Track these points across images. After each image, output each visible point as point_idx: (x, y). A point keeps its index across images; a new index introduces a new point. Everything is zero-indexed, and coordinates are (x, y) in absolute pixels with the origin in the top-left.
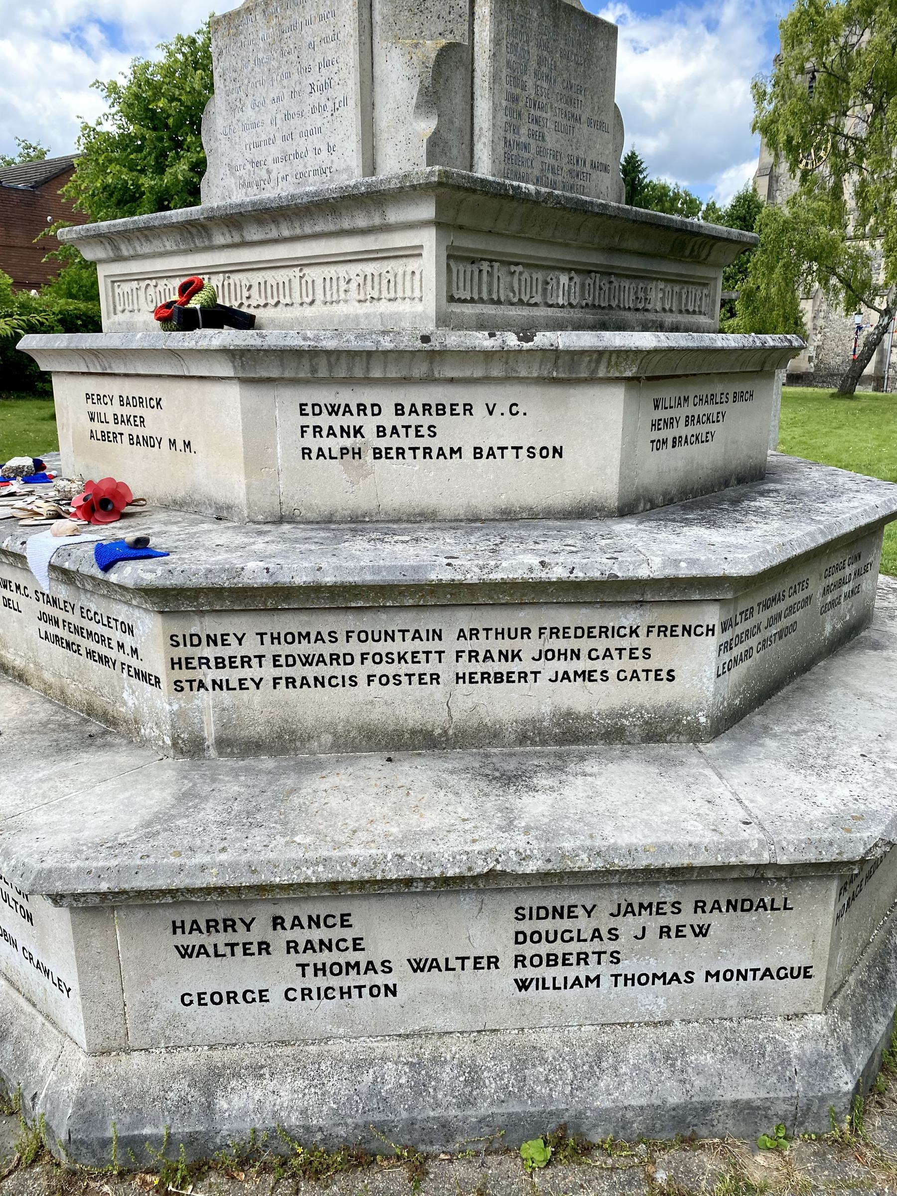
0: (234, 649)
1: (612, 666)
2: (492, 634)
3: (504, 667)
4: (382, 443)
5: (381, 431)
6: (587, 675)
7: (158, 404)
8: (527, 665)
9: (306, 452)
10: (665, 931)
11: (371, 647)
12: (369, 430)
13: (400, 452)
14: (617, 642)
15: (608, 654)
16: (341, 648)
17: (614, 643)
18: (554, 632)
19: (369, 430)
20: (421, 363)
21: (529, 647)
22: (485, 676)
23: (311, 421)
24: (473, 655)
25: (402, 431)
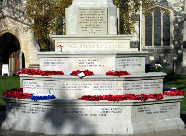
4: (126, 64)
7: (97, 60)
14: (156, 84)
16: (136, 85)
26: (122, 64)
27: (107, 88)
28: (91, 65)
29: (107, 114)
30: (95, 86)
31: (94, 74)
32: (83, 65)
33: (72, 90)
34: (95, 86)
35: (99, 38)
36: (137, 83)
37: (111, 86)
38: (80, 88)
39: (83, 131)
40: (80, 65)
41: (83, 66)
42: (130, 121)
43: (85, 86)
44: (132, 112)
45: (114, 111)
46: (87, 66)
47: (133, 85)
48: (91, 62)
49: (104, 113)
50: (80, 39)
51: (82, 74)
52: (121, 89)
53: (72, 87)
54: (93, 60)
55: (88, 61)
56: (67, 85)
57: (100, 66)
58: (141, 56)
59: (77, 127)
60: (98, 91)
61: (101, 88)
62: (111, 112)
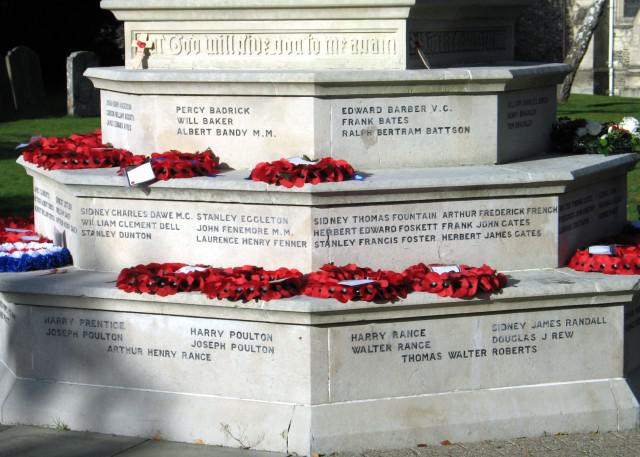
0: (343, 225)
1: (513, 229)
2: (459, 215)
3: (464, 231)
5: (381, 120)
6: (502, 235)
7: (246, 111)
8: (474, 230)
10: (554, 336)
11: (404, 223)
12: (376, 121)
13: (391, 131)
14: (514, 217)
15: (510, 224)
16: (390, 223)
17: (513, 217)
18: (487, 213)
19: (376, 121)
21: (476, 220)
22: (456, 236)
24: (450, 225)
25: (391, 121)
26: (359, 128)
27: (248, 235)
28: (222, 127)
29: (215, 353)
30: (203, 222)
31: (231, 166)
32: (194, 127)
33: (117, 235)
34: (203, 222)
35: (281, 14)
36: (401, 217)
37: (263, 226)
38: (146, 231)
39: (123, 423)
40: (182, 126)
41: (191, 131)
42: (304, 395)
43: (164, 221)
44: (318, 355)
45: (242, 341)
46: (207, 132)
47: (374, 224)
48: (220, 116)
49: (205, 349)
50: (210, 17)
51: (144, 173)
52: (304, 243)
53: (117, 223)
54: (231, 110)
55: (212, 111)
56: (99, 212)
57: (256, 132)
58: (466, 89)
59: (101, 403)
60: (216, 245)
61: (226, 234)
62: (228, 346)
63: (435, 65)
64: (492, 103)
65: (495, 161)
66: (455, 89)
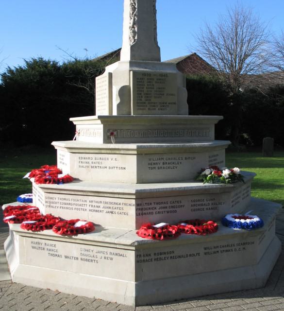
0: (54, 200)
1: (117, 211)
3: (97, 209)
4: (93, 165)
5: (92, 162)
6: (112, 212)
8: (101, 209)
9: (80, 166)
10: (105, 258)
11: (75, 202)
12: (90, 162)
13: (96, 167)
15: (115, 208)
16: (70, 202)
17: (117, 206)
18: (106, 203)
19: (90, 162)
20: (99, 151)
21: (102, 205)
22: (94, 210)
23: (81, 160)
36: (74, 200)
47: (65, 201)
63: (116, 143)
64: (134, 159)
65: (136, 182)
66: (117, 152)
